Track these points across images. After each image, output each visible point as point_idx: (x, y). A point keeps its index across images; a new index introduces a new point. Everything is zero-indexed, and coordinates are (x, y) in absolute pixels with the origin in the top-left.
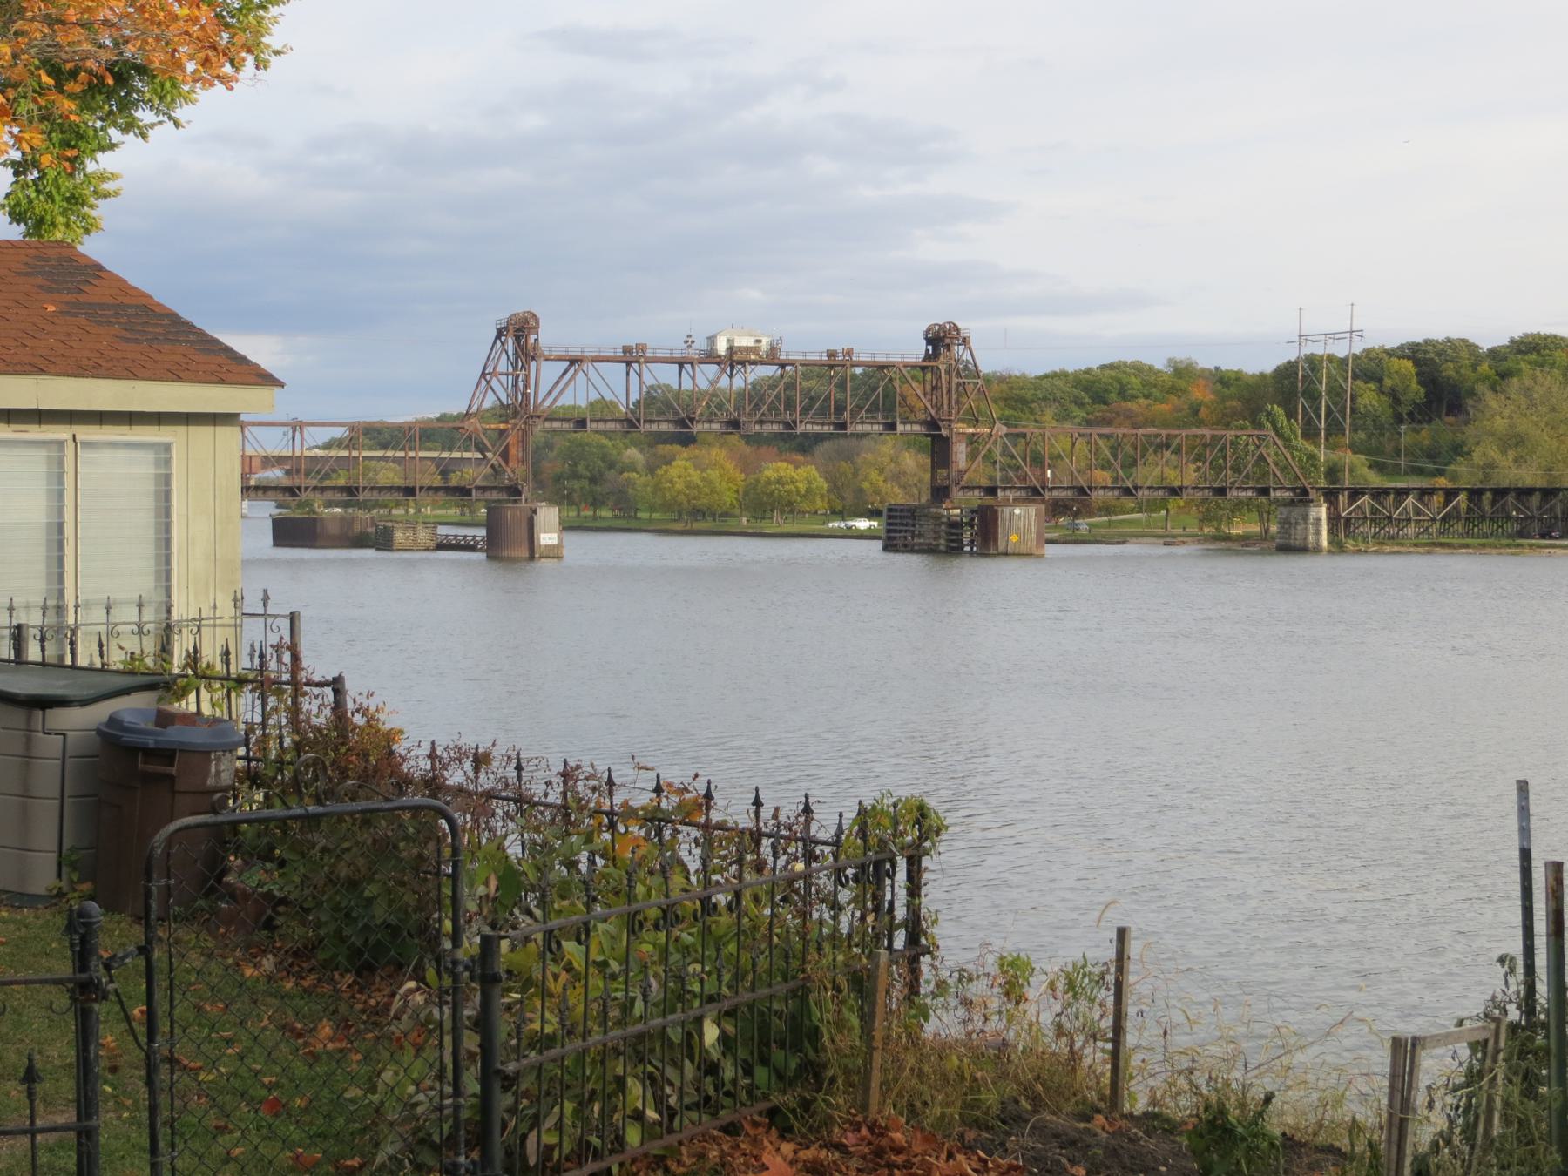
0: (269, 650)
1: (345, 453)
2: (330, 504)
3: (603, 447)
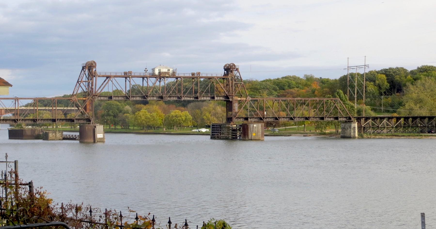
0: (8, 173)
1: (32, 108)
2: (27, 125)
3: (118, 105)
